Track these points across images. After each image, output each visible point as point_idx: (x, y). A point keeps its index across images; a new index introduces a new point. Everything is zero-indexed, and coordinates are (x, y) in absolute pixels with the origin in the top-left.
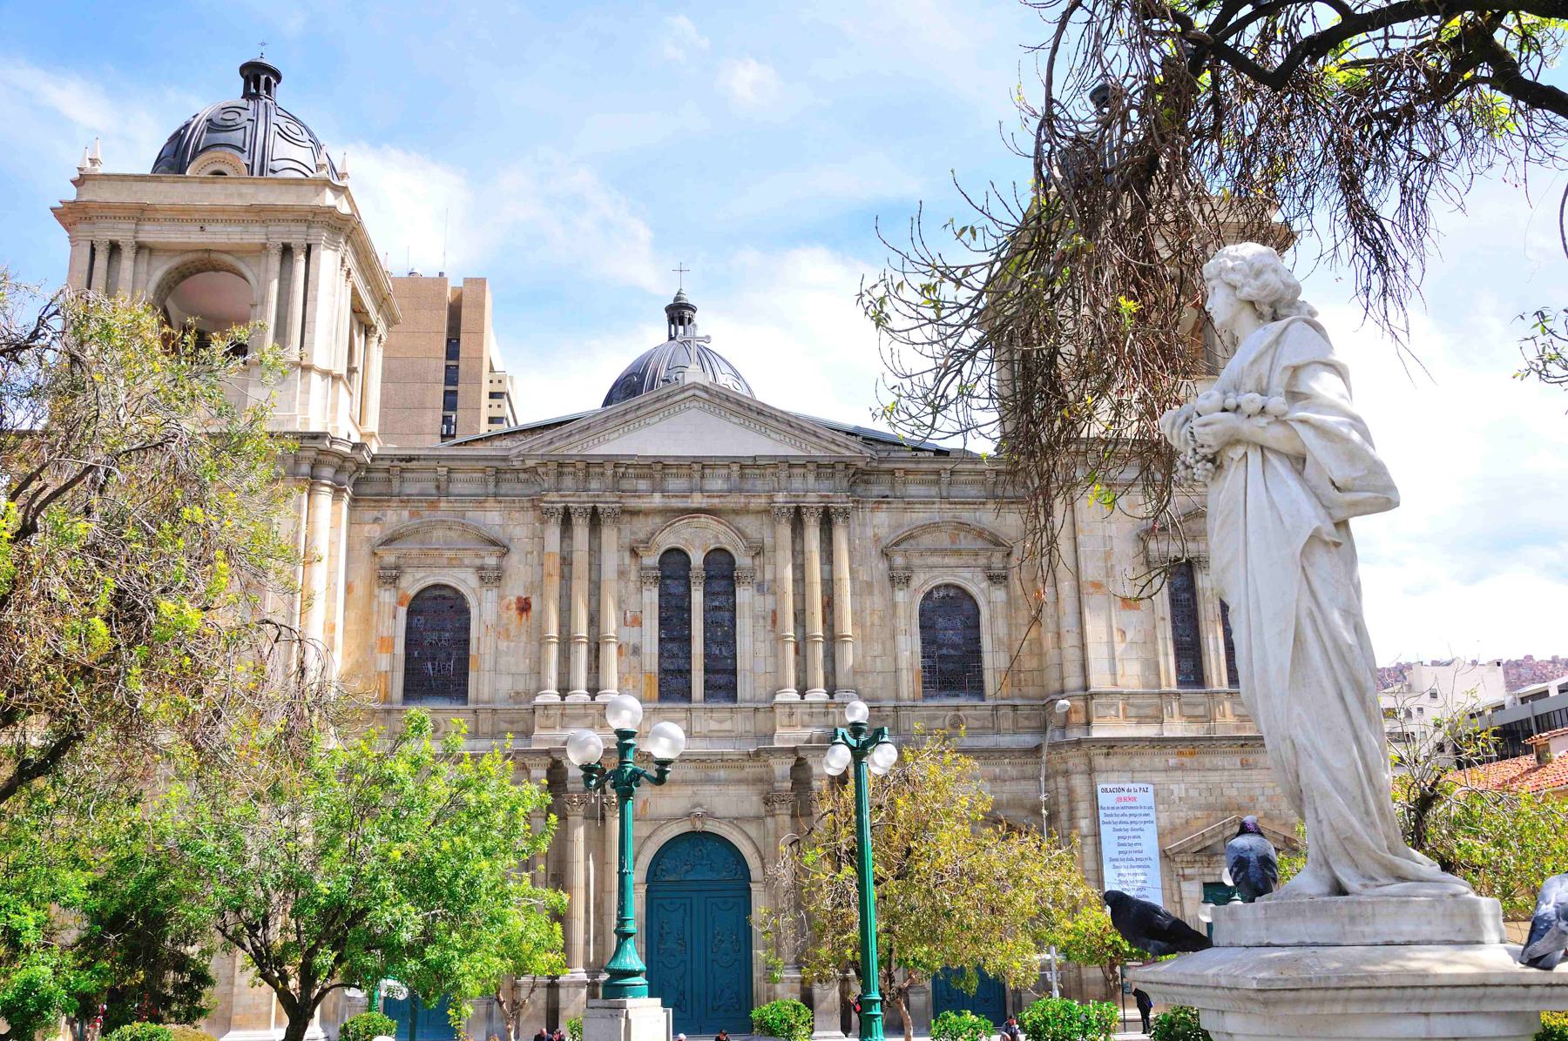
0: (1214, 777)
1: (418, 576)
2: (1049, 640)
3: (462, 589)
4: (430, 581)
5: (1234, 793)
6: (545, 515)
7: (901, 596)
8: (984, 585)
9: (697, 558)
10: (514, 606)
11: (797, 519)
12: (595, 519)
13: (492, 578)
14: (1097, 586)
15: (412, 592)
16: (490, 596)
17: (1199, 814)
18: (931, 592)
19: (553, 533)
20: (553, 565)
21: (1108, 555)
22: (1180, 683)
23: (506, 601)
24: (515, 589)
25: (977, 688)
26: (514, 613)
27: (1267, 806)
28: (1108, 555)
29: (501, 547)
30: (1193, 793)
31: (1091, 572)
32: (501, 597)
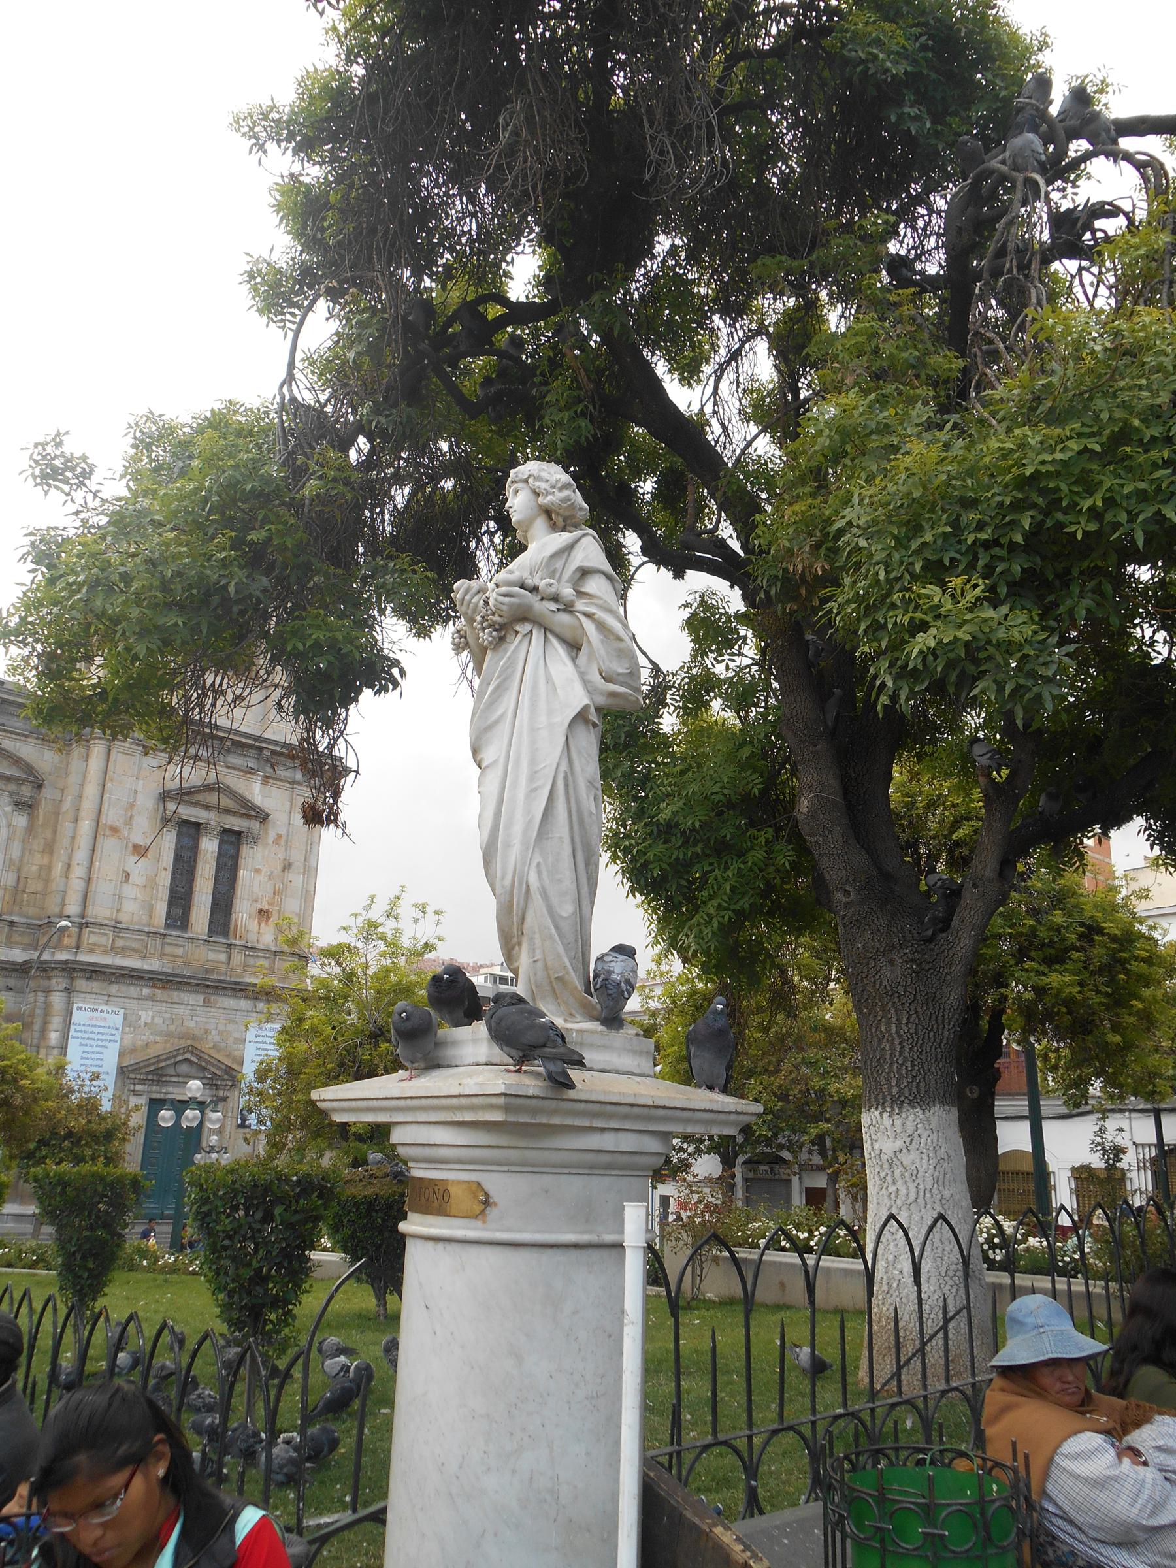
0: (179, 1010)
2: (58, 868)
5: (192, 1024)
8: (8, 809)
14: (114, 830)
17: (158, 1039)
21: (132, 805)
22: (167, 926)
27: (217, 1038)
28: (132, 805)
30: (158, 1020)
31: (112, 816)
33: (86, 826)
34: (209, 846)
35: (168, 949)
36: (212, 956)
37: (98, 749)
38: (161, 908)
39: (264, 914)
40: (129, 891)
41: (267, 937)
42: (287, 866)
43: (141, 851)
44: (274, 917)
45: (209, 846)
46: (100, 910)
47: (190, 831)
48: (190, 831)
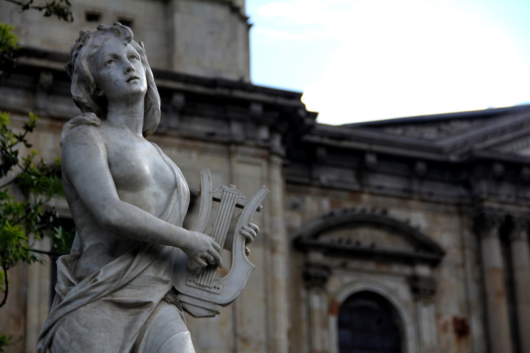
1: (348, 279)
3: (394, 300)
4: (360, 287)
6: (479, 225)
10: (451, 328)
13: (423, 291)
16: (426, 312)
19: (493, 249)
20: (496, 283)
23: (442, 321)
24: (451, 307)
26: (451, 335)
29: (432, 254)
32: (438, 316)
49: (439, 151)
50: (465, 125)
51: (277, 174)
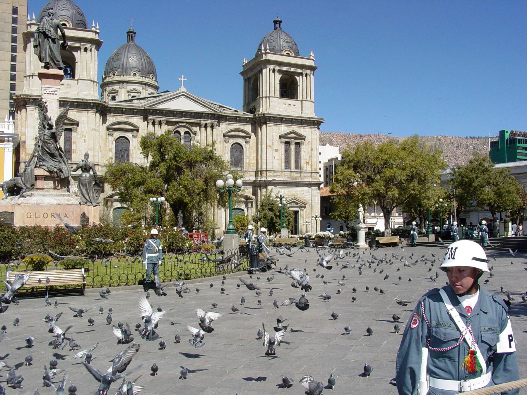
7: (227, 145)
9: (182, 133)
11: (206, 127)
12: (160, 124)
14: (270, 146)
15: (116, 138)
18: (233, 145)
25: (242, 167)
33: (264, 146)
34: (293, 147)
35: (286, 174)
36: (296, 175)
37: (264, 126)
38: (283, 164)
39: (307, 163)
40: (275, 161)
41: (309, 170)
42: (312, 150)
43: (276, 151)
44: (310, 163)
45: (293, 147)
46: (269, 168)
47: (288, 143)
48: (288, 143)
49: (139, 107)
50: (152, 98)
51: (98, 115)
